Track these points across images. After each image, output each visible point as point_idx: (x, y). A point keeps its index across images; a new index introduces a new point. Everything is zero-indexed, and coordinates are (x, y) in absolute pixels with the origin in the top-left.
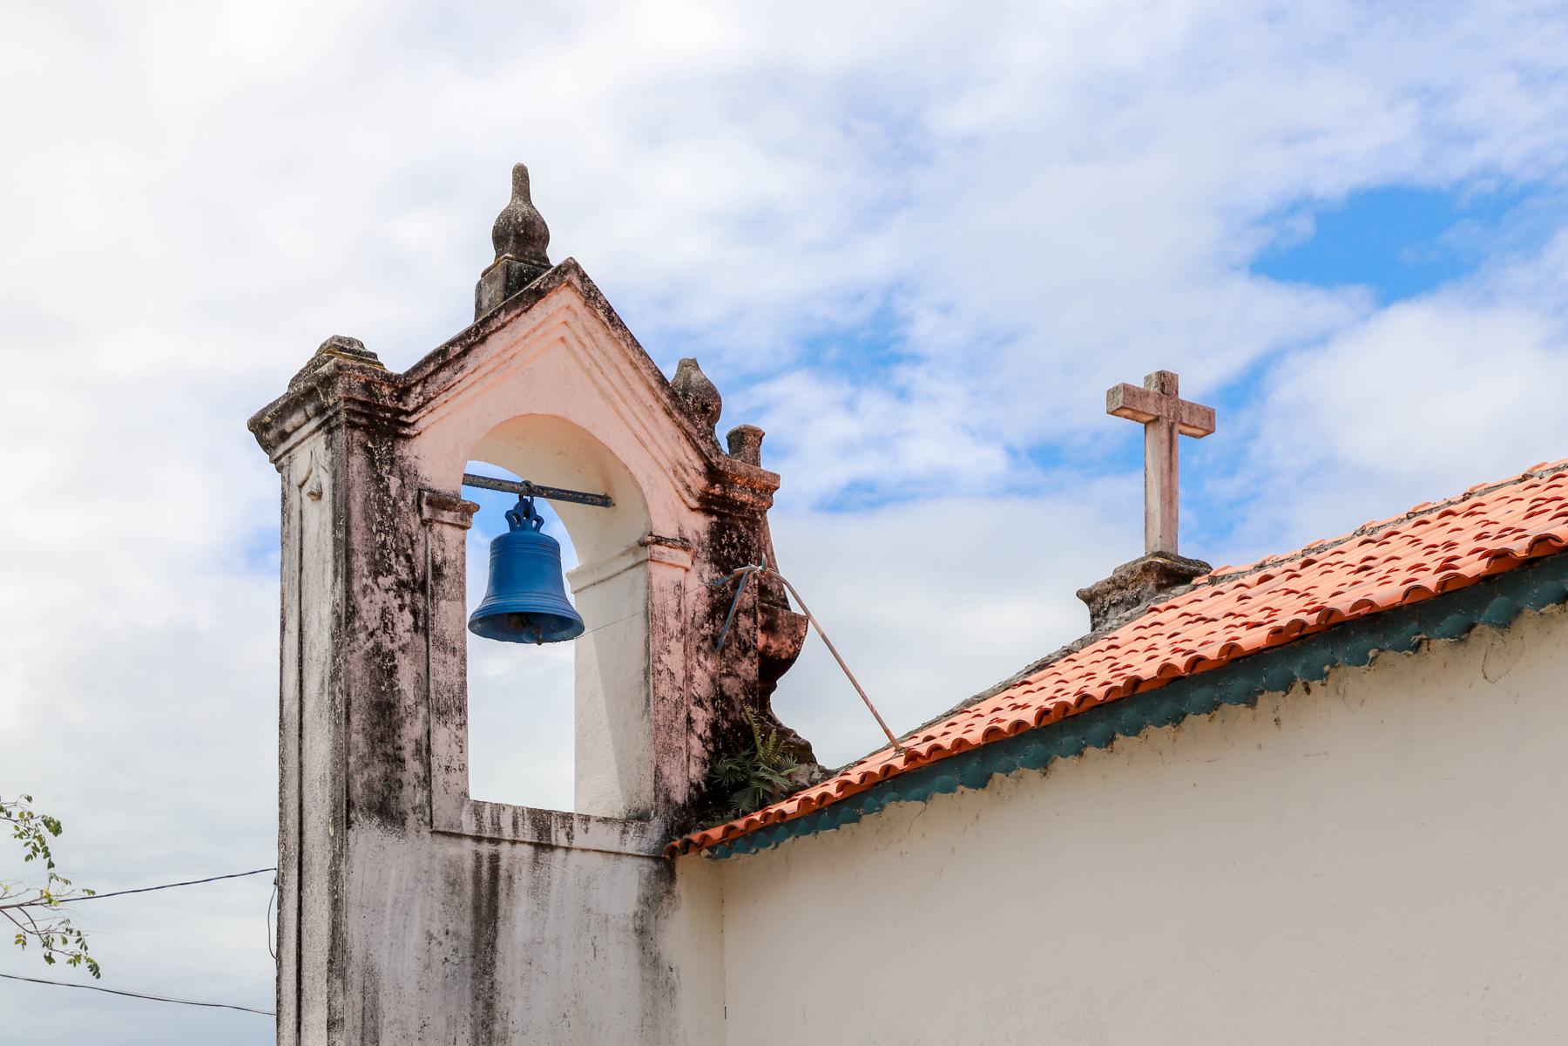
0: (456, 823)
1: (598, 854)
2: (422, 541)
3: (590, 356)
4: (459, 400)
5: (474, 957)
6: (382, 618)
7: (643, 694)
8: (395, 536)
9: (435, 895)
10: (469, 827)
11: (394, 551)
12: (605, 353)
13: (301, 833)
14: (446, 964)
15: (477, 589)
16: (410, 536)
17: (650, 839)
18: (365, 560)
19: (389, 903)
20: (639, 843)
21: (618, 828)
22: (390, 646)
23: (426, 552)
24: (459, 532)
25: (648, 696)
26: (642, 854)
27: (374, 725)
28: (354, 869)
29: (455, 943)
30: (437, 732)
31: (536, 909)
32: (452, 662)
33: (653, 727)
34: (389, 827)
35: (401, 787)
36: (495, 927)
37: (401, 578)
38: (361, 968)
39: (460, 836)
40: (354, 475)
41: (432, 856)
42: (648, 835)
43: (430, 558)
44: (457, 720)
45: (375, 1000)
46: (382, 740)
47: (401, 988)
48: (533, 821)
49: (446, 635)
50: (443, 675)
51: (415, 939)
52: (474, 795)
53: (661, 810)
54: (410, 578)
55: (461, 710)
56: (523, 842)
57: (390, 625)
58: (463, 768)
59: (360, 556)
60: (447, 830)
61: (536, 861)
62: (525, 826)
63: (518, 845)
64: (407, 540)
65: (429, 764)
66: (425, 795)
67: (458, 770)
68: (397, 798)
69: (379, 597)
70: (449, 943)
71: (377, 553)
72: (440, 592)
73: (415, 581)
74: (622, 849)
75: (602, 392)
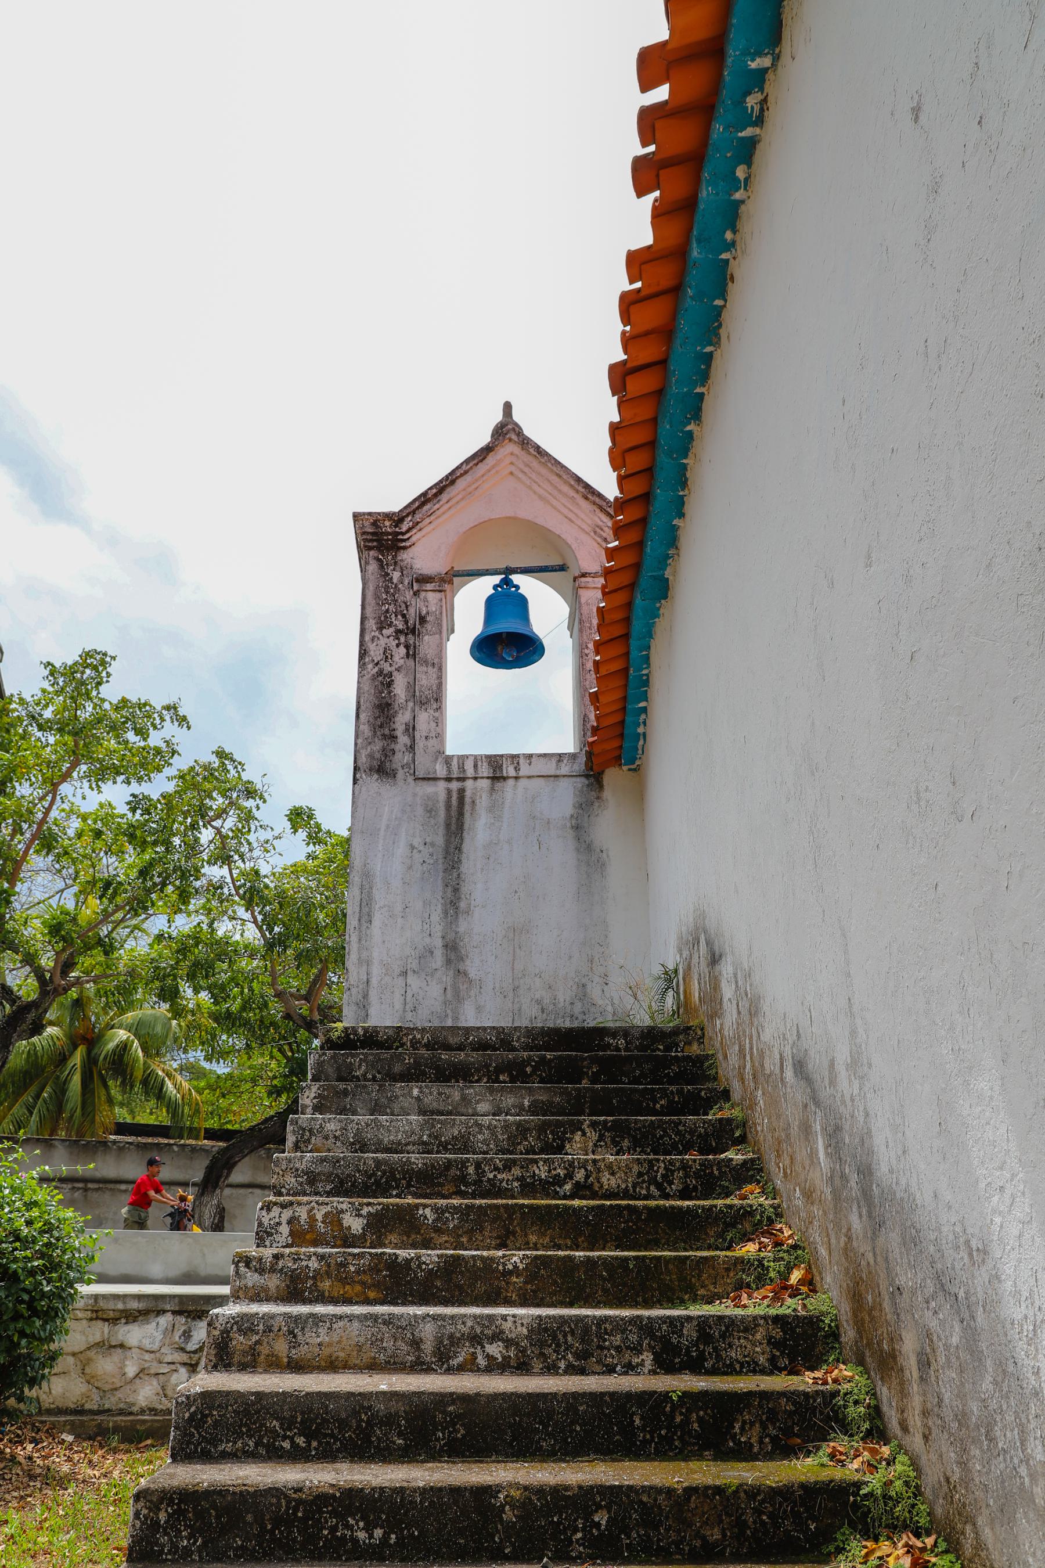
4: (440, 520)
6: (384, 653)
9: (417, 820)
10: (441, 770)
16: (405, 603)
18: (374, 622)
19: (383, 830)
22: (390, 669)
24: (438, 595)
27: (376, 718)
28: (358, 809)
29: (431, 850)
35: (394, 754)
41: (415, 795)
44: (435, 706)
45: (370, 894)
46: (381, 726)
48: (489, 763)
49: (428, 656)
50: (425, 679)
52: (449, 752)
54: (405, 626)
56: (482, 778)
60: (425, 776)
61: (492, 789)
63: (479, 780)
64: (403, 606)
69: (383, 641)
70: (426, 851)
73: (408, 628)
74: (558, 773)
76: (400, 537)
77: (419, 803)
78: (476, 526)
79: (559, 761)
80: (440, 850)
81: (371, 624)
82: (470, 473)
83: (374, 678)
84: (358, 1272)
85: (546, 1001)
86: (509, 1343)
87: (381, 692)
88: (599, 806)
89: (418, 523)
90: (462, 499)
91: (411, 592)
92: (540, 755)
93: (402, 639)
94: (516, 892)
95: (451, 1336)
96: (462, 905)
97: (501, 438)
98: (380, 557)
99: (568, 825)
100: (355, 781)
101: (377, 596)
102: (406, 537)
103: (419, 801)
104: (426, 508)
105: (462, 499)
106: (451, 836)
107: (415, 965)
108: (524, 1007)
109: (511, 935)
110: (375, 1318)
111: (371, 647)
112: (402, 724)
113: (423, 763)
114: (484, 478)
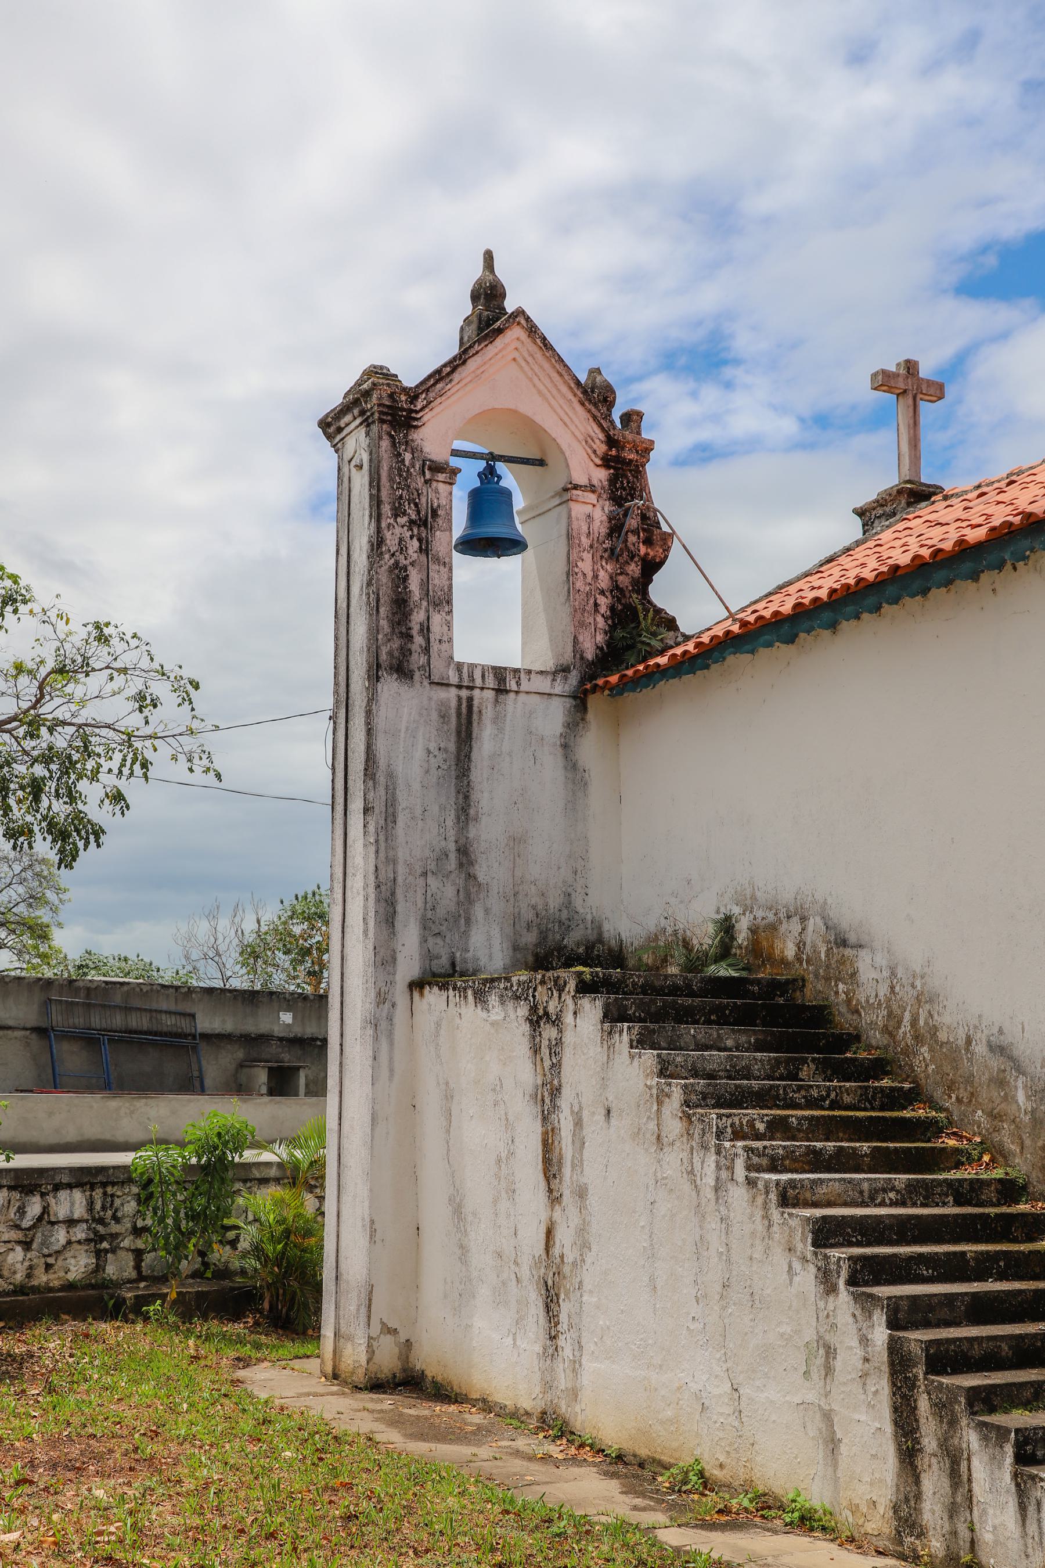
0: (446, 677)
2: (425, 494)
3: (532, 369)
5: (457, 765)
6: (399, 545)
7: (566, 588)
10: (454, 679)
12: (541, 367)
13: (348, 686)
15: (459, 523)
16: (417, 491)
18: (389, 507)
19: (403, 730)
21: (550, 678)
24: (448, 487)
25: (569, 589)
27: (394, 614)
33: (572, 610)
35: (411, 654)
39: (448, 685)
41: (430, 699)
42: (569, 681)
44: (446, 609)
45: (394, 794)
46: (399, 623)
48: (495, 674)
50: (437, 580)
51: (419, 753)
53: (578, 665)
55: (449, 602)
56: (489, 688)
58: (450, 640)
61: (496, 701)
63: (485, 690)
64: (416, 493)
65: (429, 639)
69: (398, 530)
70: (441, 756)
73: (420, 519)
74: (552, 692)
75: (539, 392)
76: (413, 415)
81: (386, 509)
83: (391, 570)
84: (800, 1155)
85: (540, 907)
86: (898, 1192)
88: (584, 727)
93: (416, 531)
94: (515, 803)
95: (875, 1189)
96: (472, 812)
97: (511, 320)
98: (393, 433)
99: (558, 743)
101: (391, 480)
102: (419, 416)
103: (433, 705)
105: (470, 381)
107: (432, 866)
108: (523, 911)
109: (512, 844)
110: (844, 1180)
111: (388, 535)
112: (417, 623)
113: (437, 666)
114: (492, 361)
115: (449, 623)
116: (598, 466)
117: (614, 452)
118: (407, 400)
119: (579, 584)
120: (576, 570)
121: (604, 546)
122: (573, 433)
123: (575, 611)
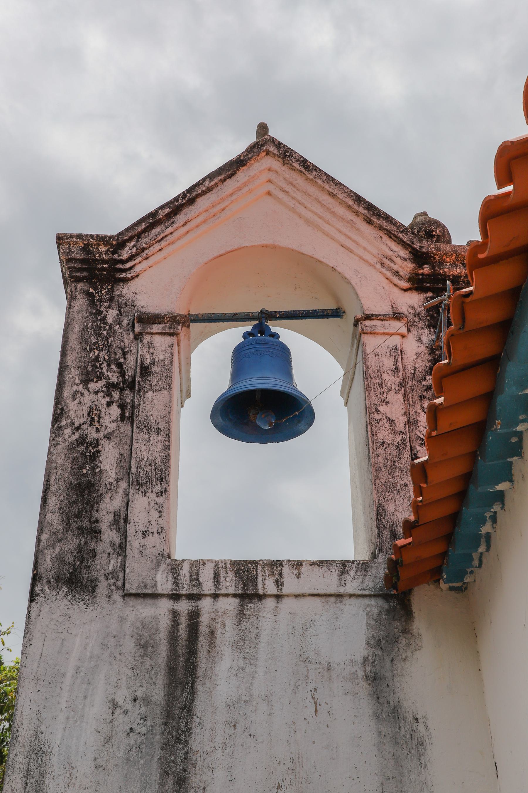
1: (317, 599)
3: (294, 198)
5: (166, 724)
6: (89, 415)
8: (108, 351)
9: (124, 660)
11: (107, 362)
12: (305, 193)
14: (131, 734)
16: (123, 349)
17: (375, 577)
18: (77, 372)
19: (69, 675)
20: (363, 582)
22: (95, 435)
23: (137, 358)
24: (168, 340)
26: (367, 592)
27: (71, 504)
28: (33, 642)
29: (143, 710)
30: (135, 501)
31: (241, 664)
32: (156, 441)
34: (77, 596)
35: (94, 556)
36: (192, 687)
37: (111, 381)
38: (27, 749)
39: (155, 596)
40: (75, 314)
41: (122, 620)
43: (139, 362)
44: (158, 489)
46: (78, 516)
47: (73, 768)
48: (237, 574)
49: (152, 419)
52: (178, 555)
54: (121, 379)
56: (226, 595)
57: (96, 418)
59: (73, 370)
60: (139, 591)
61: (241, 613)
62: (228, 579)
63: (221, 599)
64: (121, 352)
65: (126, 532)
66: (119, 560)
67: (156, 533)
68: (89, 567)
69: (88, 399)
71: (90, 365)
72: (147, 386)
73: (124, 382)
74: (342, 590)
75: (308, 222)
77: (128, 632)
78: (221, 256)
79: (343, 572)
80: (158, 710)
82: (215, 190)
83: (72, 448)
87: (82, 468)
88: (408, 645)
89: (144, 249)
90: (204, 222)
91: (132, 336)
92: (313, 564)
93: (116, 396)
98: (91, 290)
99: (361, 673)
100: (33, 597)
101: (83, 339)
103: (128, 629)
104: (155, 231)
105: (204, 222)
106: (175, 688)
111: (72, 406)
112: (108, 513)
114: (234, 197)
115: (161, 506)
116: (405, 290)
117: (426, 269)
118: (108, 250)
119: (383, 434)
120: (377, 417)
121: (424, 383)
122: (361, 258)
123: (378, 470)
